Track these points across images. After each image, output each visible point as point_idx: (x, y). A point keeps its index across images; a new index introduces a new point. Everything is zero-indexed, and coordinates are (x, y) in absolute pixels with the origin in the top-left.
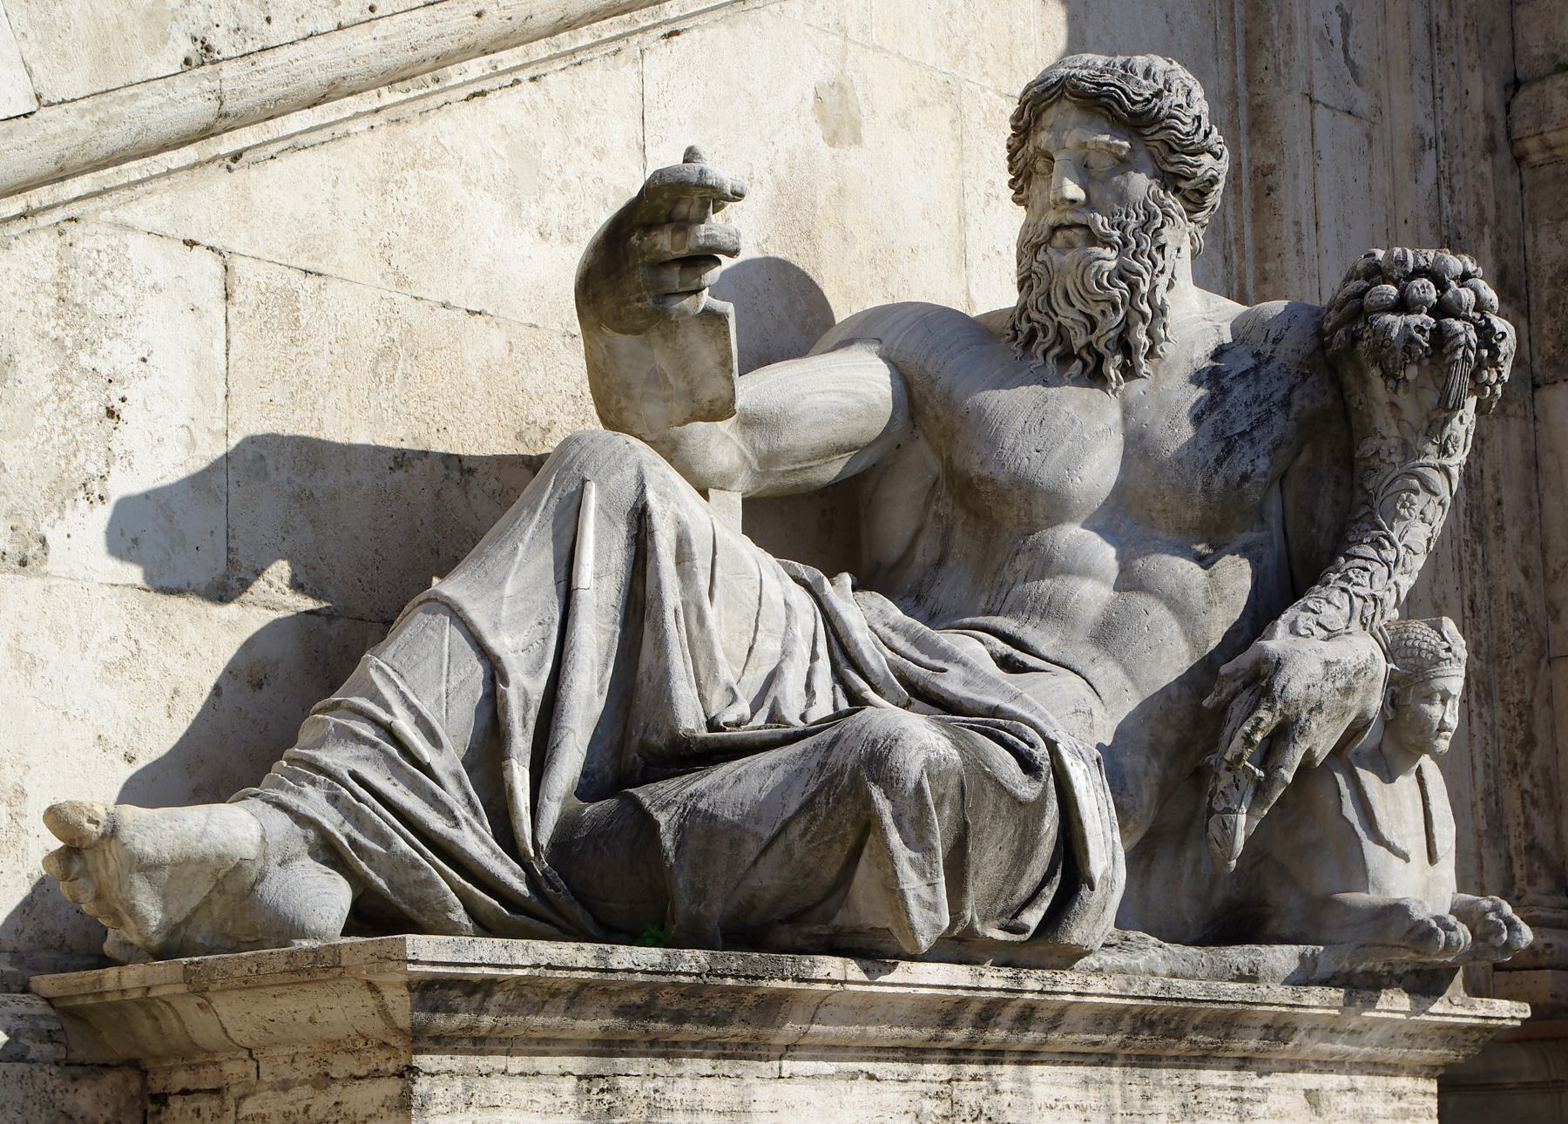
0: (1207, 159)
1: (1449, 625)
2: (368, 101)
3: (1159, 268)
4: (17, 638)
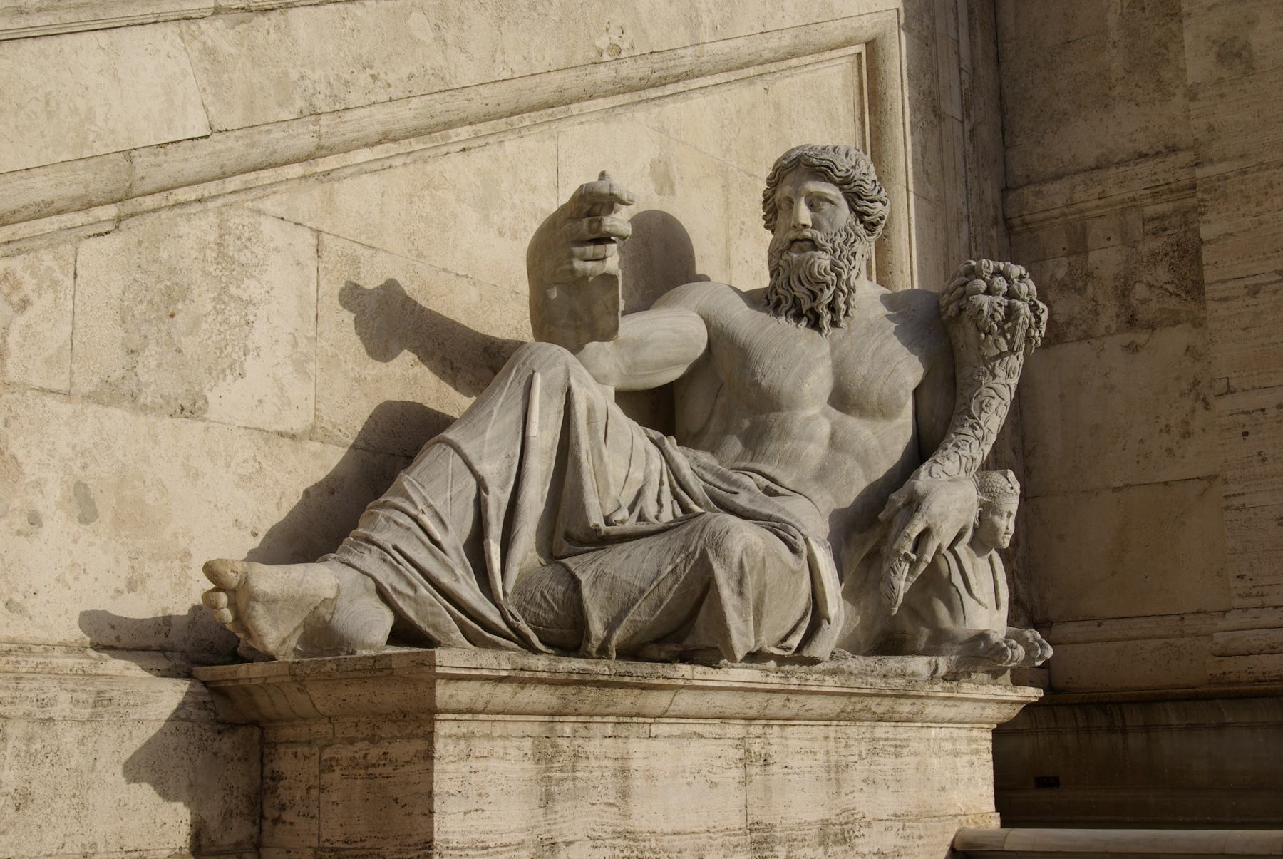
0: (879, 205)
1: (1011, 474)
2: (402, 147)
4: (188, 458)
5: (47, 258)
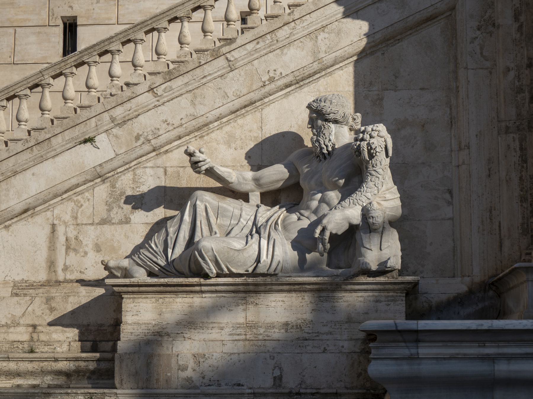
0: (332, 115)
3: (325, 137)
5: (87, 194)
